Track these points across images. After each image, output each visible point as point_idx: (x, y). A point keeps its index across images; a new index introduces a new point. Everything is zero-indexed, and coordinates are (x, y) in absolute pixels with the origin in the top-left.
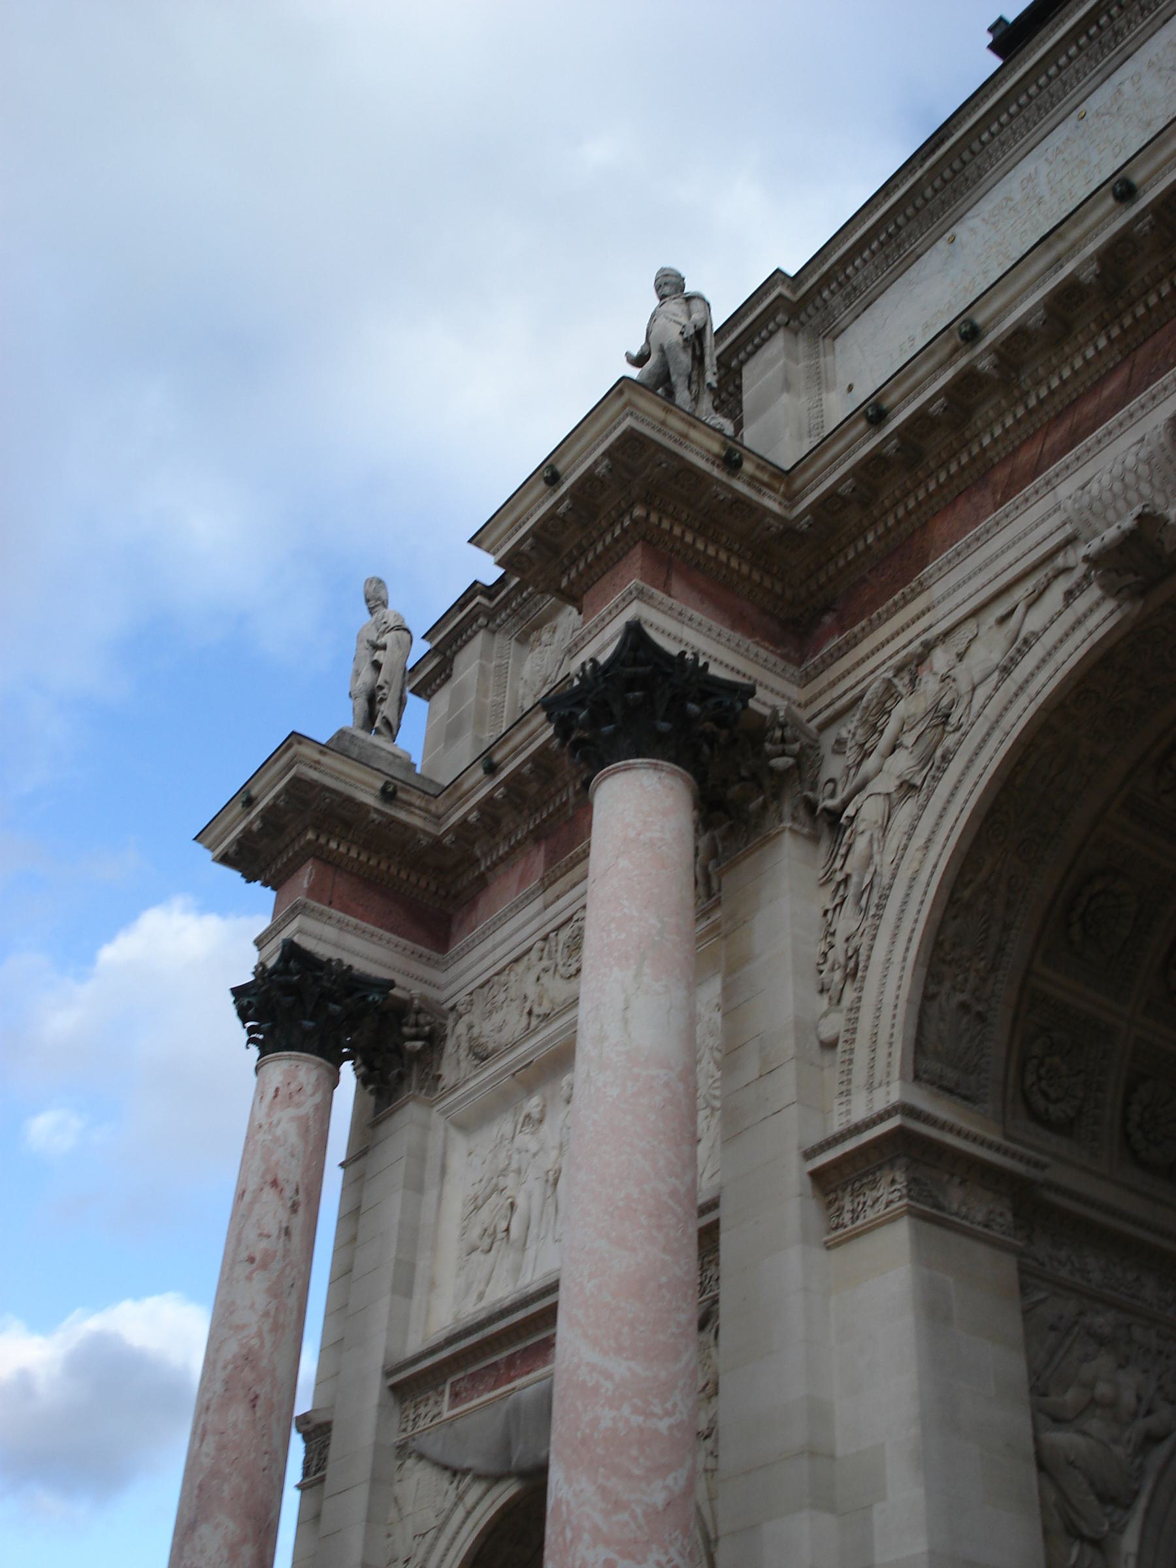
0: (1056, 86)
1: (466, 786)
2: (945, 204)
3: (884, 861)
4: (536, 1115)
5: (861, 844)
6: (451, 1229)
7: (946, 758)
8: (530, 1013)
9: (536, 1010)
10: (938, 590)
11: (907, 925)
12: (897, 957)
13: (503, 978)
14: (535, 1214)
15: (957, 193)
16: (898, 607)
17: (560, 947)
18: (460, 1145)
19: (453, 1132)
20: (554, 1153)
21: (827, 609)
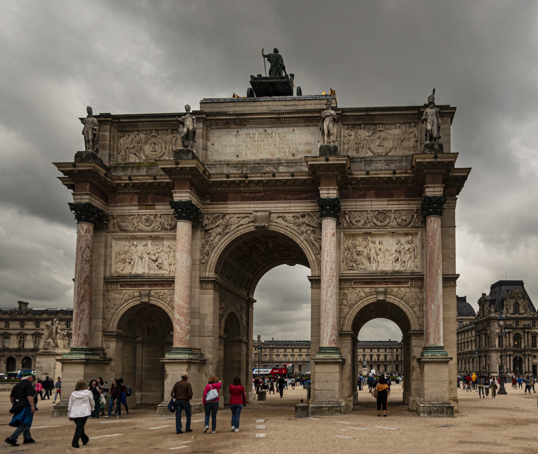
0: (264, 122)
2: (239, 125)
3: (214, 242)
4: (136, 245)
5: (211, 238)
6: (113, 256)
7: (227, 233)
8: (135, 227)
9: (137, 227)
10: (229, 206)
11: (217, 253)
12: (215, 256)
13: (127, 217)
14: (136, 262)
15: (241, 125)
16: (222, 204)
17: (143, 220)
18: (114, 243)
19: (113, 239)
20: (141, 254)
21: (208, 194)
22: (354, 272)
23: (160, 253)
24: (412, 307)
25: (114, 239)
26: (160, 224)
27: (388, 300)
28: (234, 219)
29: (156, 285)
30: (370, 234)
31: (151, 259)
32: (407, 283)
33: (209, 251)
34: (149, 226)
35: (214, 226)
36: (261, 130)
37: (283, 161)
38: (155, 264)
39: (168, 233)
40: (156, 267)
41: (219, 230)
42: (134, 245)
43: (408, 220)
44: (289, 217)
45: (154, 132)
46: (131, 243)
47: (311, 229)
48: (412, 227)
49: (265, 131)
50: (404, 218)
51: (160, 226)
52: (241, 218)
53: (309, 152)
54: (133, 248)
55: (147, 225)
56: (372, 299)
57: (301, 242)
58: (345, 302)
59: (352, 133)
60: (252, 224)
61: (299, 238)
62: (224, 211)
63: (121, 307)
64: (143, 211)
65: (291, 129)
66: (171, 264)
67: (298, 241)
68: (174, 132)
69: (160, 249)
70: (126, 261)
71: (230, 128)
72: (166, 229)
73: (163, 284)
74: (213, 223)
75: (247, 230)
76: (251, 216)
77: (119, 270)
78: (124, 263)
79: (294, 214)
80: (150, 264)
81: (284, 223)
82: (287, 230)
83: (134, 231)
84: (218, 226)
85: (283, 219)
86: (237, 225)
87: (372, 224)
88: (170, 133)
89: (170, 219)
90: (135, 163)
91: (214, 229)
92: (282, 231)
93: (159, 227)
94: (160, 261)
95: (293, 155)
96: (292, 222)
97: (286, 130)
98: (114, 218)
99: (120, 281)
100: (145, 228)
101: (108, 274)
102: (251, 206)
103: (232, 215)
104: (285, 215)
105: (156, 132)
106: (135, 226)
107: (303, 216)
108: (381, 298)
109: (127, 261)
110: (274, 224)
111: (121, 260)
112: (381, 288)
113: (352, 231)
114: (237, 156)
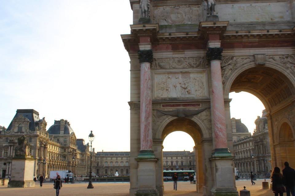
1: (165, 34)
3: (228, 75)
4: (171, 78)
5: (226, 72)
6: (155, 86)
7: (236, 69)
10: (236, 51)
13: (164, 59)
17: (176, 61)
23: (189, 83)
25: (156, 74)
26: (189, 63)
28: (239, 60)
29: (188, 105)
31: (182, 87)
33: (225, 81)
34: (180, 65)
35: (226, 65)
36: (248, 5)
37: (267, 23)
38: (186, 91)
39: (194, 70)
40: (187, 93)
41: (231, 67)
42: (169, 78)
44: (277, 58)
45: (177, 6)
46: (167, 77)
47: (294, 65)
49: (251, 5)
51: (188, 65)
52: (244, 59)
53: (282, 17)
54: (169, 80)
55: (180, 64)
57: (288, 74)
60: (253, 63)
61: (286, 72)
62: (232, 54)
63: (164, 121)
64: (176, 55)
65: (268, 3)
66: (197, 91)
67: (286, 74)
68: (190, 6)
69: (188, 80)
70: (164, 89)
71: (228, 3)
72: (193, 67)
73: (194, 104)
74: (225, 63)
75: (250, 67)
76: (251, 57)
77: (160, 95)
78: (163, 90)
79: (280, 56)
80: (182, 90)
82: (277, 66)
83: (170, 69)
84: (229, 64)
85: (273, 59)
86: (242, 64)
88: (188, 7)
89: (195, 60)
90: (166, 26)
91: (227, 66)
92: (274, 67)
93: (188, 65)
94: (189, 88)
95: (272, 19)
96: (280, 61)
97: (264, 4)
98: (156, 60)
99: (162, 103)
100: (177, 66)
101: (154, 98)
102: (251, 51)
103: (238, 57)
104: (274, 57)
105: (179, 6)
106: (170, 66)
107: (287, 57)
109: (165, 89)
110: (268, 62)
111: (160, 88)
114: (235, 20)
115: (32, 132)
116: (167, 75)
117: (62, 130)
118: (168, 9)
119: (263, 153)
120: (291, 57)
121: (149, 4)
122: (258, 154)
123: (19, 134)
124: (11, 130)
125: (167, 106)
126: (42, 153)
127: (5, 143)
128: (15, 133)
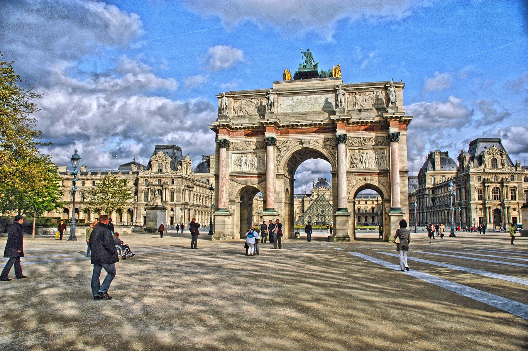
10: (290, 136)
22: (354, 169)
24: (385, 187)
27: (372, 183)
30: (362, 149)
32: (382, 174)
36: (304, 97)
41: (285, 148)
43: (382, 142)
47: (332, 147)
48: (384, 145)
50: (379, 140)
54: (242, 158)
56: (363, 183)
58: (350, 185)
59: (351, 97)
62: (287, 139)
65: (320, 95)
72: (259, 149)
81: (317, 144)
87: (363, 144)
97: (317, 96)
100: (248, 148)
102: (301, 136)
107: (327, 141)
108: (368, 182)
112: (368, 177)
113: (353, 148)
115: (174, 172)
116: (241, 154)
117: (213, 168)
118: (244, 102)
119: (466, 199)
120: (331, 140)
121: (227, 102)
122: (461, 200)
123: (159, 174)
124: (150, 170)
125: (239, 177)
126: (187, 197)
127: (143, 186)
128: (155, 173)
